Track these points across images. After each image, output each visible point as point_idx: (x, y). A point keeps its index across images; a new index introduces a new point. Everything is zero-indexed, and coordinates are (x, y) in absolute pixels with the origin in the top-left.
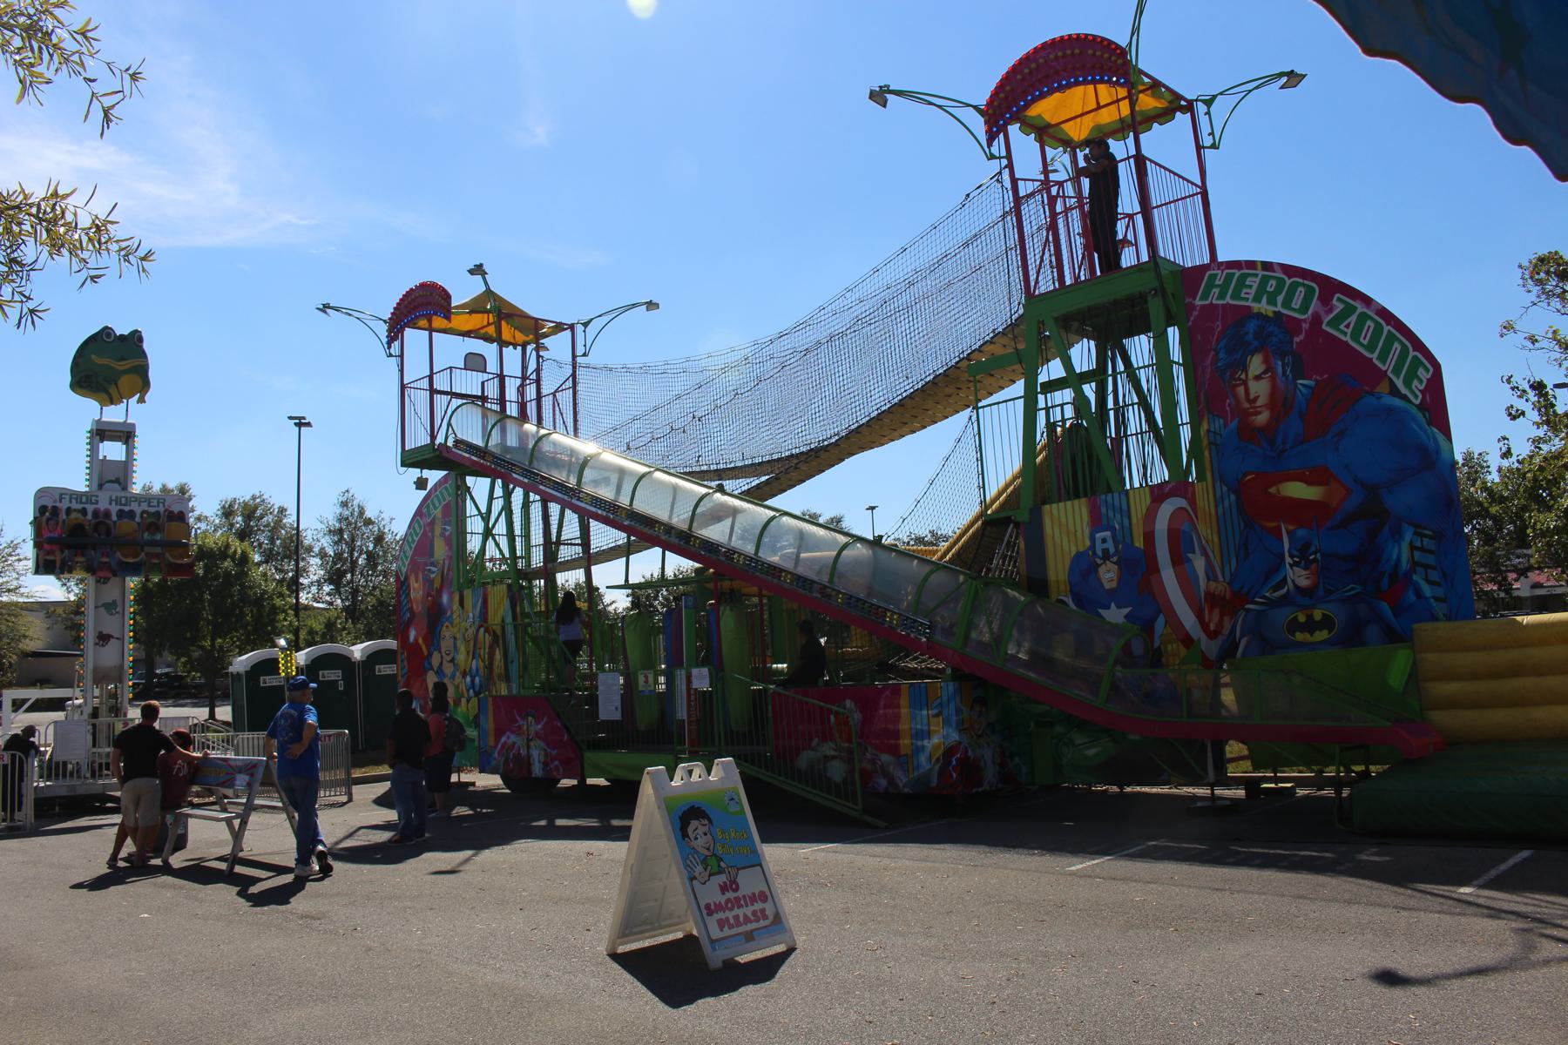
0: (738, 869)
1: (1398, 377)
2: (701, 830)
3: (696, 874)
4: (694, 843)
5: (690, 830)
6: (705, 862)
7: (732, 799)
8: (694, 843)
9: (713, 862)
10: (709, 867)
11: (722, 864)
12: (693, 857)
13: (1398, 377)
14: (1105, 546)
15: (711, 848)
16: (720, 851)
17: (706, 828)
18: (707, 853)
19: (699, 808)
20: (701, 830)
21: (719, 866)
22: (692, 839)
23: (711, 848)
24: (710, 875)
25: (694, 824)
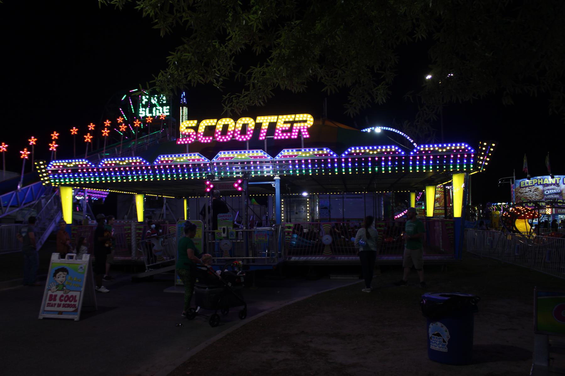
0: (70, 291)
1: (87, 156)
2: (63, 275)
3: (52, 289)
4: (57, 279)
5: (58, 275)
6: (57, 286)
7: (82, 268)
8: (57, 279)
9: (61, 287)
10: (58, 288)
11: (65, 288)
12: (54, 284)
13: (87, 156)
14: (540, 181)
15: (63, 282)
16: (66, 283)
17: (65, 275)
18: (60, 283)
19: (63, 268)
20: (63, 275)
21: (63, 288)
22: (57, 277)
23: (63, 282)
24: (57, 290)
25: (60, 273)
